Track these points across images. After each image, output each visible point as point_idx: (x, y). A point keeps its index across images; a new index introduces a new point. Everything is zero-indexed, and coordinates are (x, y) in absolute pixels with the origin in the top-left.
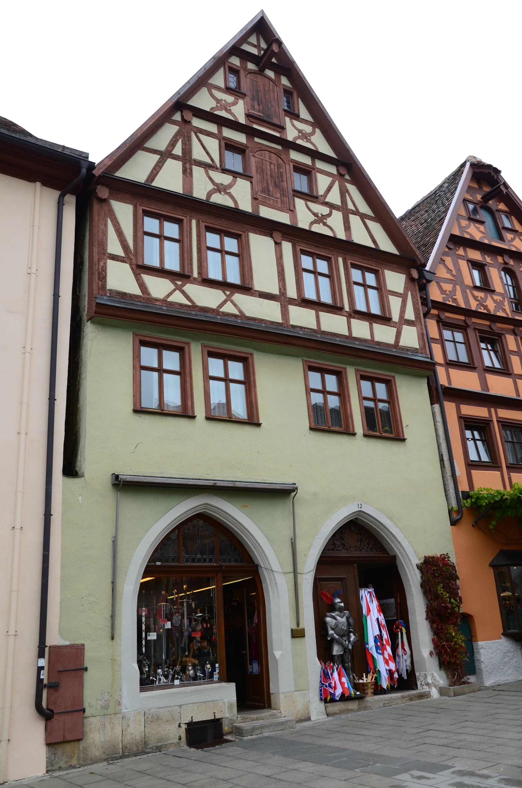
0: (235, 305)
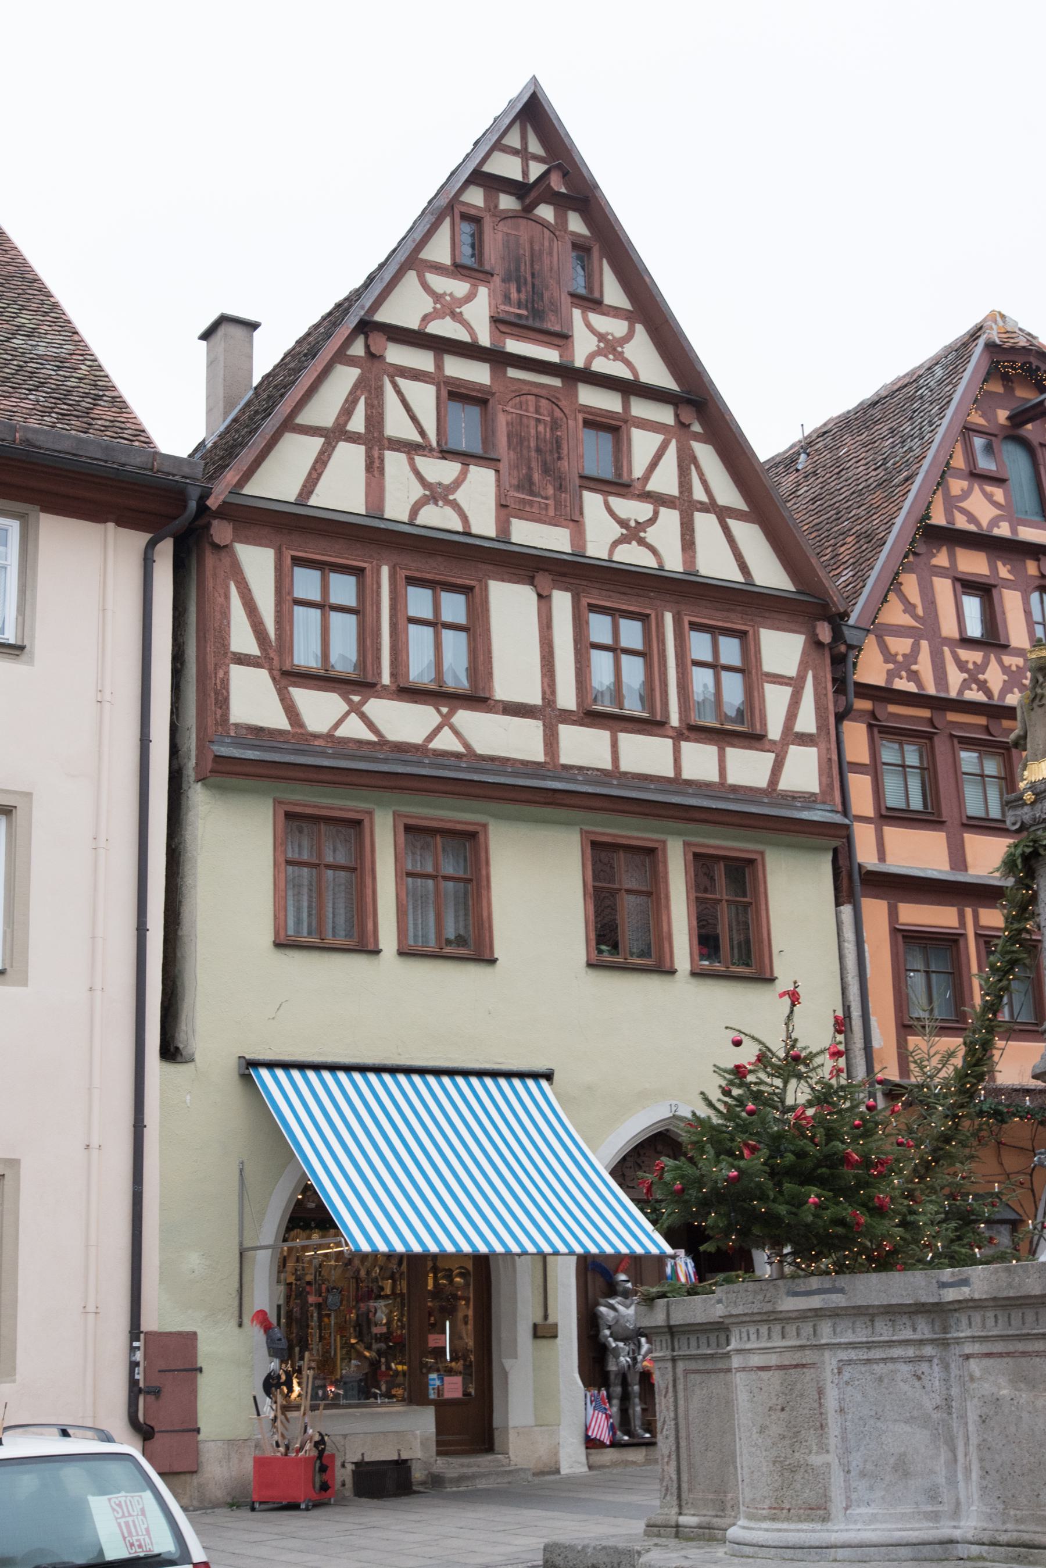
0: (457, 733)
